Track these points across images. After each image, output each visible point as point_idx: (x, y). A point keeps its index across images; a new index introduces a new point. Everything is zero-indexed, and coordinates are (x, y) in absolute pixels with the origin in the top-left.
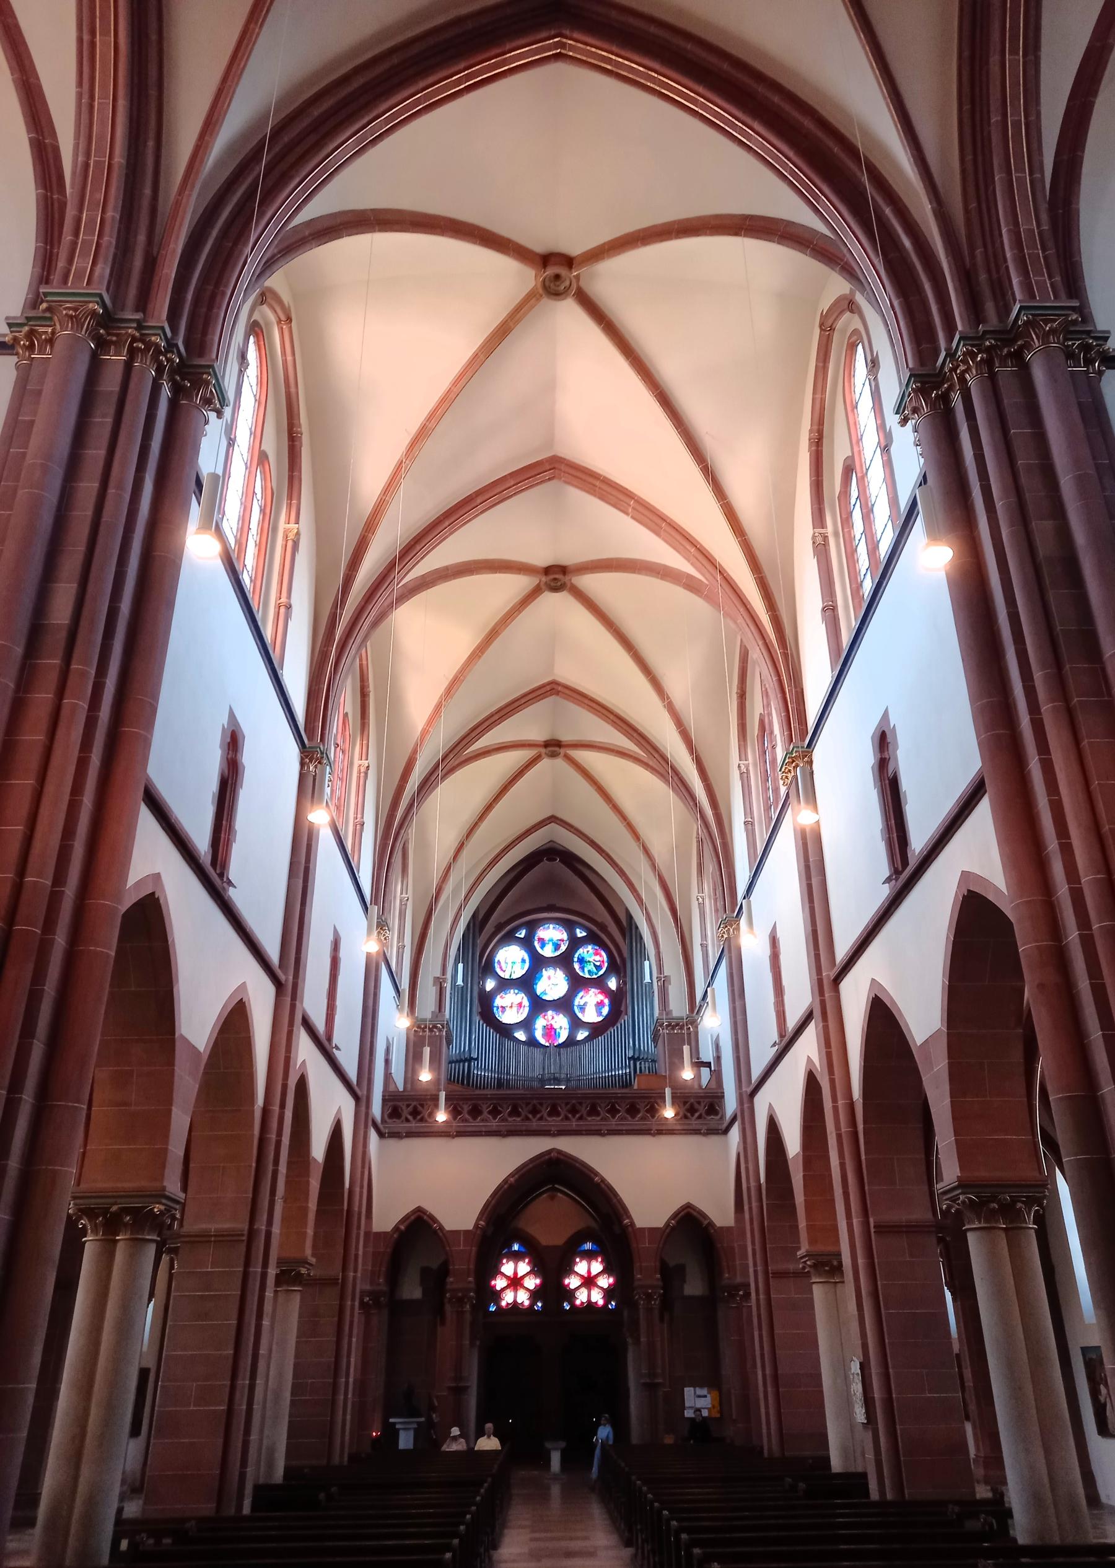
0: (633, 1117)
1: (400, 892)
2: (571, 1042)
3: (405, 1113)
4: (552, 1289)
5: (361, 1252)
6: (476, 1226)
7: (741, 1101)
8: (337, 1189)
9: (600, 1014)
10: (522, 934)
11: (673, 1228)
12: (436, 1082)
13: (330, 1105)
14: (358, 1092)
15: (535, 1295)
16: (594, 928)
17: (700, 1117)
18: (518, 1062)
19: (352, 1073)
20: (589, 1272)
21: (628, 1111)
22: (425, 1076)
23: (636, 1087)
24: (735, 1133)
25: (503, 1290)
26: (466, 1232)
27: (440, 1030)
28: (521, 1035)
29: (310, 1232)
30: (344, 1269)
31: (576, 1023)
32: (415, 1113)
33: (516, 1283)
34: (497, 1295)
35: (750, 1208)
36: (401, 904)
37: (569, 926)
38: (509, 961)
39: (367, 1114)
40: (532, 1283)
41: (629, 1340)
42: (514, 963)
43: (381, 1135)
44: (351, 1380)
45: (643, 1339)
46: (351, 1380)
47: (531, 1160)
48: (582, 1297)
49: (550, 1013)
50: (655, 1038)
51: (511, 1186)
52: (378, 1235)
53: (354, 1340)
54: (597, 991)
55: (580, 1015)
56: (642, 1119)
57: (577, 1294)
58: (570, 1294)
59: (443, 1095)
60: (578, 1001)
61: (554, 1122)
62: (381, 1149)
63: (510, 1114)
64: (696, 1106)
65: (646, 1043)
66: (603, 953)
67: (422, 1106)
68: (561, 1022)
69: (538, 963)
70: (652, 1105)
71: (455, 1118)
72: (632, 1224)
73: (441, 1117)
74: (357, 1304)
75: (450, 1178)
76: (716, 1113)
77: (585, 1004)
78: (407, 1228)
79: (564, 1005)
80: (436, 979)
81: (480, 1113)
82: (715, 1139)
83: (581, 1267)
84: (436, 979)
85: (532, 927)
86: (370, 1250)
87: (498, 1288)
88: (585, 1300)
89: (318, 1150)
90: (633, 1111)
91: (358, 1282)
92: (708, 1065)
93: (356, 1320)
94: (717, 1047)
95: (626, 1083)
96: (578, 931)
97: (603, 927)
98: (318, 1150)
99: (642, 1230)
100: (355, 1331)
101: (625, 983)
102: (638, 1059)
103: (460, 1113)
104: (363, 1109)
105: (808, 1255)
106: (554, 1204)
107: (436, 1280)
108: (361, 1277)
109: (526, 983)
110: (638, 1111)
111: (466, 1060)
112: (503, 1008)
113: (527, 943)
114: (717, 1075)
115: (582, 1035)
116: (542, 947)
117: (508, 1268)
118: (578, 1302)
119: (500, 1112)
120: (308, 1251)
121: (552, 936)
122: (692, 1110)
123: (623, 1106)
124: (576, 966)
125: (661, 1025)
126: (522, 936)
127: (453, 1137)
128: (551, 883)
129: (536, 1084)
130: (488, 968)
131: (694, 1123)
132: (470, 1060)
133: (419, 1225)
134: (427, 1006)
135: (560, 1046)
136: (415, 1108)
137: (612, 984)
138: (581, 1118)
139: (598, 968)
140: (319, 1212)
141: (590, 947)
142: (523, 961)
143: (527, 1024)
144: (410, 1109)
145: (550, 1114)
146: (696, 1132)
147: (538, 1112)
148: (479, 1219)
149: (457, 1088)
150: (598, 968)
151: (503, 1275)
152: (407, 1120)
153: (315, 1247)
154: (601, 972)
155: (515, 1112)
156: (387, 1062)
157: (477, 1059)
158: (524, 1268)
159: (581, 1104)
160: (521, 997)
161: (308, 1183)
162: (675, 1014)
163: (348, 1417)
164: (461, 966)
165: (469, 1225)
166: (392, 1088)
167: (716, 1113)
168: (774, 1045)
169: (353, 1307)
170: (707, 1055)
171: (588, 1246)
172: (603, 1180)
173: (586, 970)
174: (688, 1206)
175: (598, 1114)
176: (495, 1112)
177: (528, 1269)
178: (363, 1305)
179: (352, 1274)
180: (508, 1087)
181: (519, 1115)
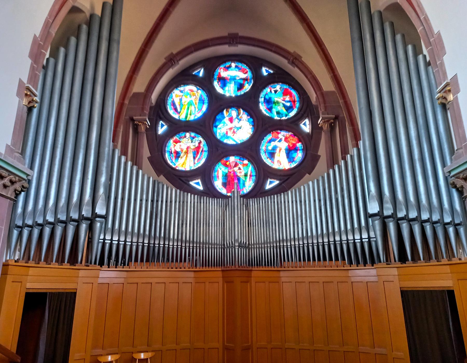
2: (258, 192)
9: (291, 159)
28: (197, 184)
31: (263, 172)
37: (254, 63)
42: (190, 104)
49: (232, 159)
54: (288, 134)
55: (268, 161)
66: (294, 92)
68: (245, 170)
69: (218, 105)
77: (275, 148)
79: (249, 150)
85: (212, 64)
97: (295, 60)
102: (393, 216)
109: (204, 127)
113: (205, 84)
115: (271, 184)
116: (222, 88)
124: (263, 108)
126: (201, 74)
137: (306, 126)
139: (289, 109)
141: (278, 87)
142: (202, 101)
143: (205, 173)
150: (289, 109)
154: (292, 114)
173: (274, 111)
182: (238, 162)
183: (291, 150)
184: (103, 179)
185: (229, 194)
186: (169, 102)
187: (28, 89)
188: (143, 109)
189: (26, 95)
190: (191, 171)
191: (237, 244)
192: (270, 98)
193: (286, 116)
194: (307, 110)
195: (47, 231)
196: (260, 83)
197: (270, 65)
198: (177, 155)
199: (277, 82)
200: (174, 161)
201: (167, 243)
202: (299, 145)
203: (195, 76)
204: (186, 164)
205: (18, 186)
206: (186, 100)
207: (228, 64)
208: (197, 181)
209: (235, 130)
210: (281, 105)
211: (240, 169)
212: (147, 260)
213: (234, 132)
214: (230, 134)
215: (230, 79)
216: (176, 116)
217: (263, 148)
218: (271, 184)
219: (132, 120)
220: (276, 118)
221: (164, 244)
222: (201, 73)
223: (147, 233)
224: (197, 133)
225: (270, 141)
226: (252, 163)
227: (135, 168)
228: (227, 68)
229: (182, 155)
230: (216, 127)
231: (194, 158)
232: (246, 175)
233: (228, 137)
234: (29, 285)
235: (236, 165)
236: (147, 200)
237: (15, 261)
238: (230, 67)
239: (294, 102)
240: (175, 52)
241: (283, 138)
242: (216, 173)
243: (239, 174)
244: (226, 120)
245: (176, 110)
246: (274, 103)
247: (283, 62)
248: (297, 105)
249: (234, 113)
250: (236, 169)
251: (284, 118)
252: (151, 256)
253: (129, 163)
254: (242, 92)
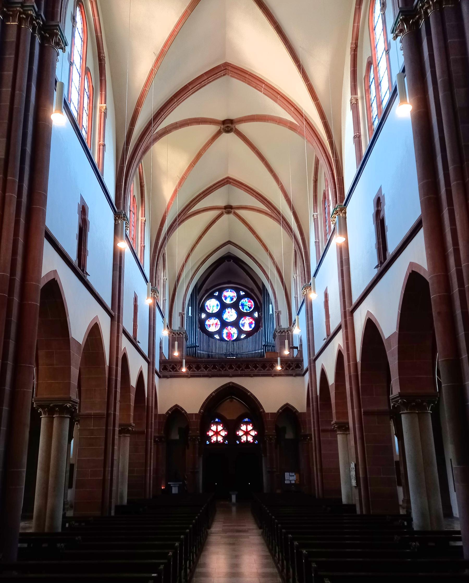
0: (264, 369)
1: (164, 277)
2: (238, 339)
3: (169, 368)
4: (232, 436)
5: (153, 422)
6: (200, 411)
7: (310, 363)
8: (142, 398)
9: (250, 327)
10: (217, 294)
11: (281, 413)
12: (181, 356)
13: (137, 365)
14: (149, 360)
15: (225, 438)
16: (248, 291)
17: (292, 369)
18: (216, 347)
19: (146, 353)
20: (247, 429)
21: (262, 367)
22: (176, 354)
23: (265, 357)
24: (307, 376)
25: (212, 436)
26: (196, 414)
27: (183, 335)
28: (217, 337)
29: (132, 414)
30: (147, 428)
31: (240, 332)
32: (173, 368)
33: (217, 433)
34: (209, 438)
35: (313, 405)
36: (164, 282)
37: (237, 290)
38: (211, 305)
39: (153, 369)
40: (223, 433)
41: (263, 455)
42: (213, 306)
43: (160, 377)
44: (152, 468)
45: (268, 455)
46: (152, 468)
47: (222, 386)
48: (244, 439)
49: (229, 327)
50: (274, 337)
51: (213, 396)
52: (160, 415)
53: (152, 454)
54: (249, 318)
55: (242, 328)
56: (268, 370)
57: (242, 438)
58: (239, 438)
59: (184, 361)
60: (241, 322)
61: (231, 371)
62: (160, 382)
63: (213, 368)
64: (291, 365)
65: (270, 339)
66: (252, 302)
67: (176, 365)
68: (234, 331)
69: (224, 306)
70: (272, 363)
71: (190, 370)
72: (264, 411)
73: (184, 370)
74: (153, 441)
75: (189, 393)
76: (300, 367)
78: (172, 412)
79: (235, 324)
80: (180, 313)
81: (200, 368)
82: (298, 378)
83: (244, 428)
84: (180, 313)
85: (221, 291)
86: (157, 421)
87: (210, 435)
88: (245, 440)
89: (133, 382)
90: (264, 367)
91: (153, 433)
92: (297, 348)
93: (153, 447)
94: (301, 340)
95: (262, 356)
96: (241, 292)
97: (252, 290)
98: (133, 382)
99: (268, 413)
100: (152, 451)
101: (261, 314)
102: (267, 345)
103: (192, 368)
104: (151, 367)
105: (336, 423)
106: (231, 403)
107: (184, 432)
108: (153, 431)
110: (266, 367)
111: (194, 347)
112: (209, 325)
113: (219, 298)
114: (300, 352)
115: (243, 336)
117: (214, 428)
118: (242, 441)
119: (208, 368)
120: (132, 421)
121: (229, 295)
122: (289, 366)
123: (261, 365)
124: (240, 307)
125: (277, 332)
126: (217, 295)
127: (189, 377)
128: (229, 272)
129: (224, 357)
130: (203, 309)
131: (290, 372)
132: (196, 347)
133: (177, 411)
134: (176, 326)
135: (234, 341)
136: (173, 366)
137: (256, 315)
138: (242, 370)
139: (250, 308)
140: (135, 407)
141: (246, 299)
142: (217, 305)
143: (220, 332)
144: (171, 366)
145: (229, 369)
146: (291, 375)
147: (225, 367)
148: (201, 409)
149: (191, 358)
151: (212, 430)
152: (170, 371)
153: (134, 420)
154: (251, 310)
155: (214, 368)
156: (161, 348)
157: (199, 346)
158: (220, 428)
159: (242, 364)
160: (217, 321)
161: (130, 395)
162: (283, 327)
163: (152, 482)
164: (190, 308)
165: (197, 412)
166: (163, 358)
167: (300, 367)
168: (324, 339)
169: (151, 442)
170: (296, 344)
171: (246, 420)
172: (252, 394)
174: (287, 404)
175: (249, 368)
176: (206, 368)
177: (222, 428)
178: (155, 441)
179: (150, 430)
180: (212, 358)
181: (216, 369)
183: (250, 324)
196: (240, 298)
197: (243, 291)
217: (240, 323)
218: (243, 336)
220: (245, 311)
240: (208, 288)
248: (253, 306)
254: (232, 302)
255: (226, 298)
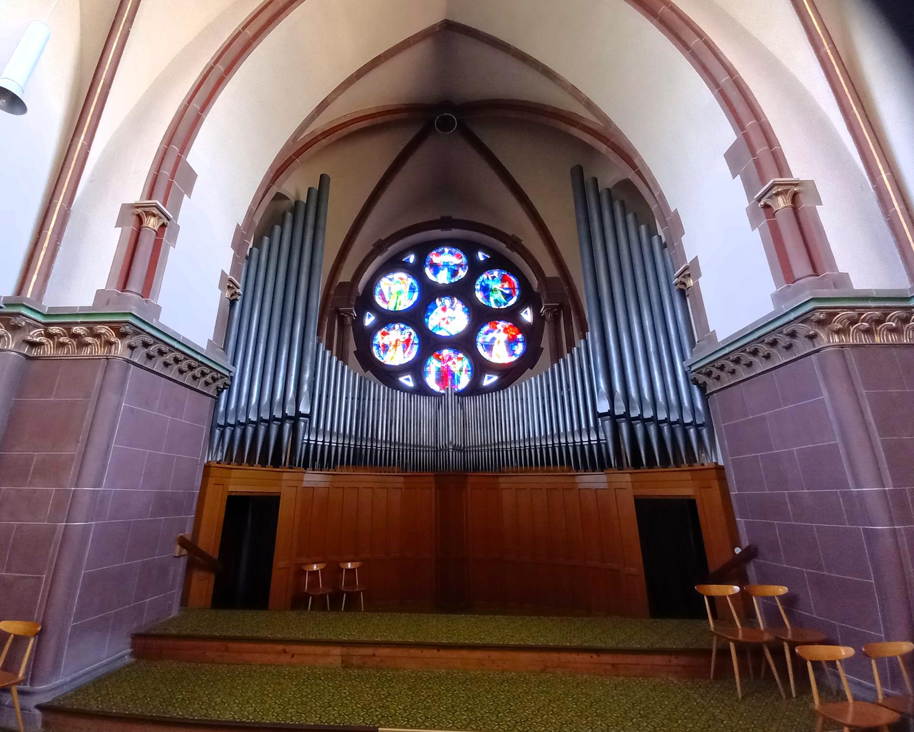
2: (475, 389)
9: (512, 353)
28: (407, 381)
31: (480, 367)
37: (468, 248)
42: (400, 293)
49: (446, 352)
54: (507, 325)
55: (485, 355)
60: (481, 338)
66: (513, 279)
69: (429, 294)
77: (494, 339)
79: (465, 343)
85: (424, 250)
97: (515, 244)
113: (416, 272)
115: (489, 380)
121: (446, 264)
124: (479, 296)
135: (462, 394)
139: (508, 297)
142: (412, 289)
143: (416, 368)
150: (508, 297)
154: (512, 302)
173: (492, 299)
182: (452, 355)
184: (307, 375)
185: (443, 391)
186: (378, 290)
187: (231, 281)
188: (349, 299)
189: (229, 287)
190: (401, 365)
191: (451, 447)
192: (487, 285)
193: (505, 304)
194: (528, 298)
195: (250, 430)
196: (476, 269)
197: (486, 249)
198: (385, 348)
199: (495, 268)
200: (382, 354)
201: (374, 445)
202: (520, 336)
203: (407, 263)
204: (396, 357)
205: (220, 384)
206: (395, 289)
207: (440, 250)
208: (406, 377)
209: (449, 320)
210: (500, 293)
211: (454, 363)
212: (354, 464)
213: (447, 323)
214: (443, 324)
215: (444, 266)
216: (384, 306)
217: (480, 339)
218: (489, 380)
219: (337, 311)
220: (494, 306)
221: (372, 446)
222: (412, 258)
223: (354, 434)
224: (407, 324)
225: (487, 333)
226: (467, 357)
227: (340, 363)
228: (439, 254)
229: (391, 348)
230: (428, 317)
231: (404, 351)
232: (461, 370)
233: (440, 329)
234: (231, 488)
235: (450, 358)
236: (353, 398)
237: (218, 463)
238: (443, 252)
239: (514, 289)
241: (502, 329)
242: (428, 368)
243: (453, 369)
244: (439, 310)
245: (384, 299)
246: (492, 290)
247: (502, 246)
248: (517, 293)
249: (447, 302)
250: (450, 363)
251: (503, 307)
252: (358, 458)
253: (335, 359)
255: (436, 268)
